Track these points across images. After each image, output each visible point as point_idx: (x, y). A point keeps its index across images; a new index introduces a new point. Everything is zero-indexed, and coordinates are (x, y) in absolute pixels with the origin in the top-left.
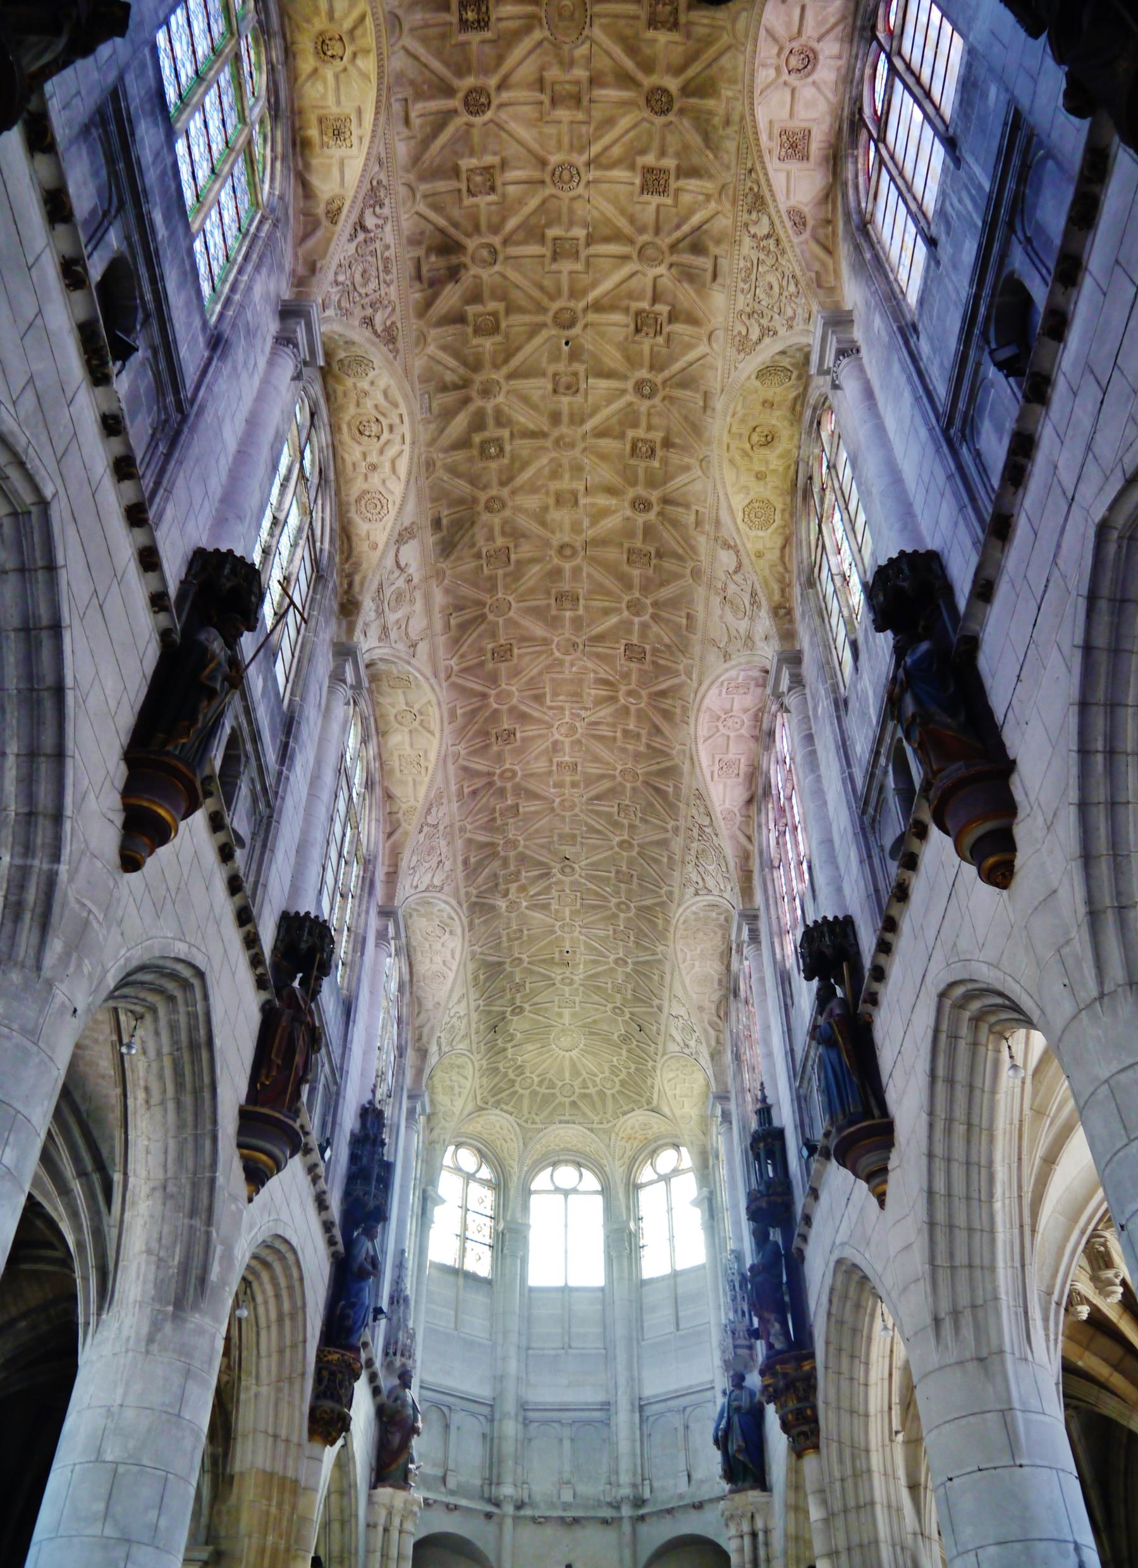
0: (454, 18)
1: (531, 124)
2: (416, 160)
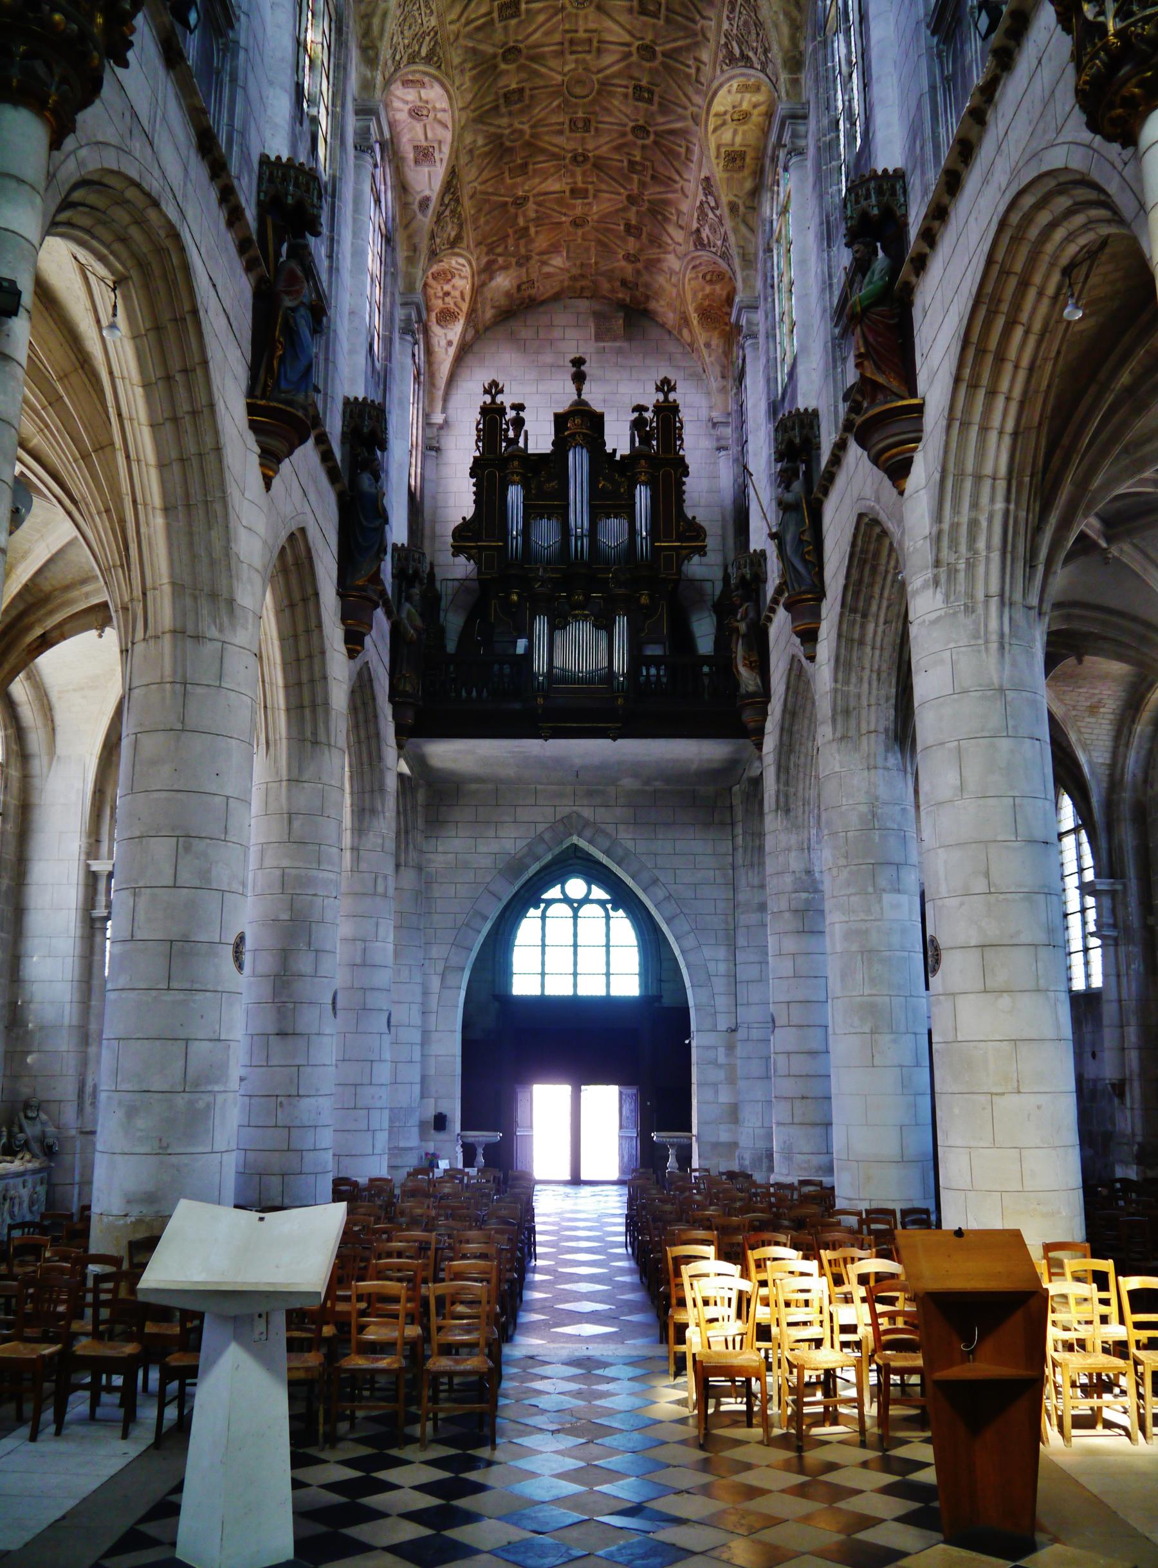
0: (656, 99)
1: (610, 31)
2: (697, 44)
